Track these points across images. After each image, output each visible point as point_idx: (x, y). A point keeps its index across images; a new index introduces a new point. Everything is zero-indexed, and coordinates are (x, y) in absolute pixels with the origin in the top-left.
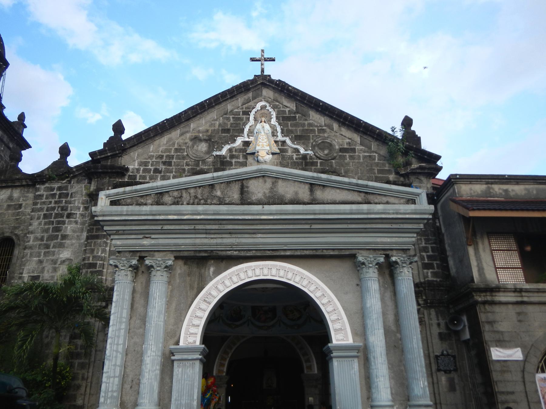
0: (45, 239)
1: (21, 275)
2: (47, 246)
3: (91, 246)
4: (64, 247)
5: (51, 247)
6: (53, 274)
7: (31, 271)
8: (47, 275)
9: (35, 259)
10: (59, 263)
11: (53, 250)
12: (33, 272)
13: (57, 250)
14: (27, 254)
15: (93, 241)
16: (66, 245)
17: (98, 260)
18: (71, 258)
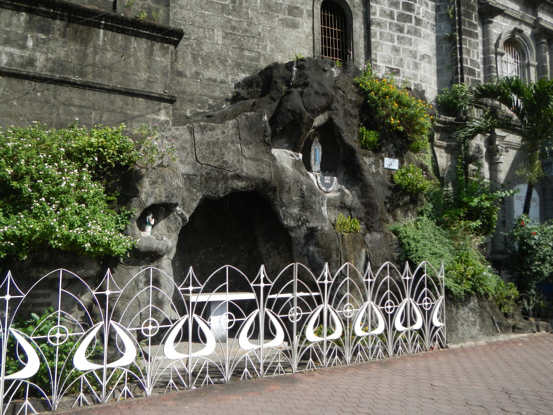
0: (396, 17)
1: (375, 63)
2: (401, 30)
3: (466, 45)
4: (420, 36)
5: (406, 31)
6: (415, 72)
7: (387, 60)
8: (407, 70)
9: (387, 43)
10: (419, 58)
11: (409, 36)
12: (389, 62)
13: (413, 37)
14: (376, 33)
15: (468, 38)
16: (422, 34)
17: (475, 66)
18: (429, 55)
